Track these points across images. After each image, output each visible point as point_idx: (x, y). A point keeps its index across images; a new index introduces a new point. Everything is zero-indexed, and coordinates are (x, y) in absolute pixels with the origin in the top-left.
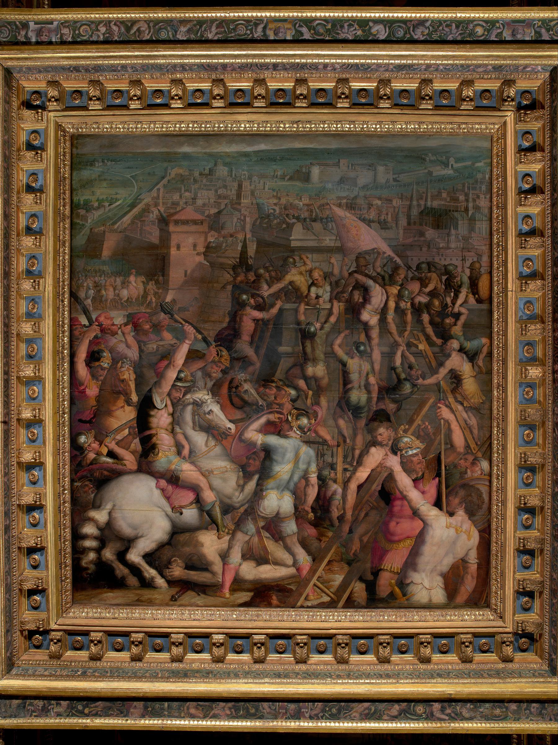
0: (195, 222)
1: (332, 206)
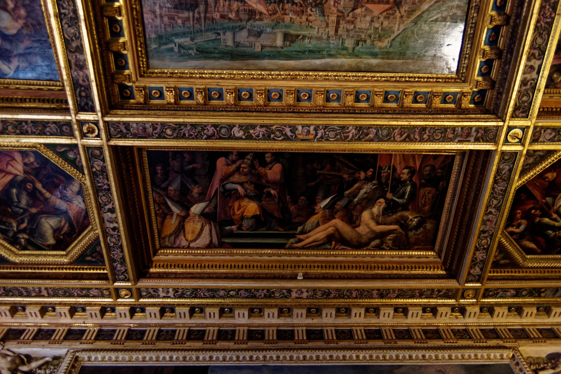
1: (267, 13)
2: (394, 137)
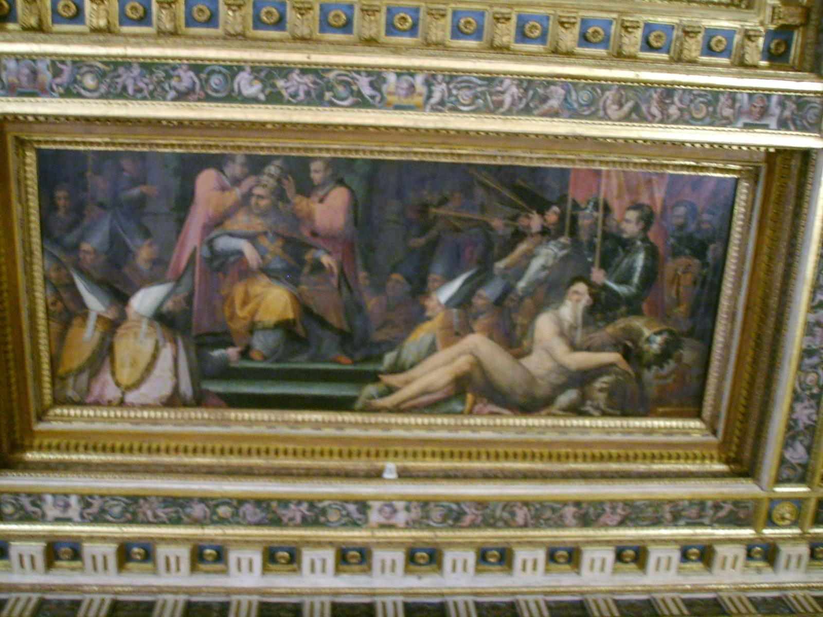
2: (605, 109)
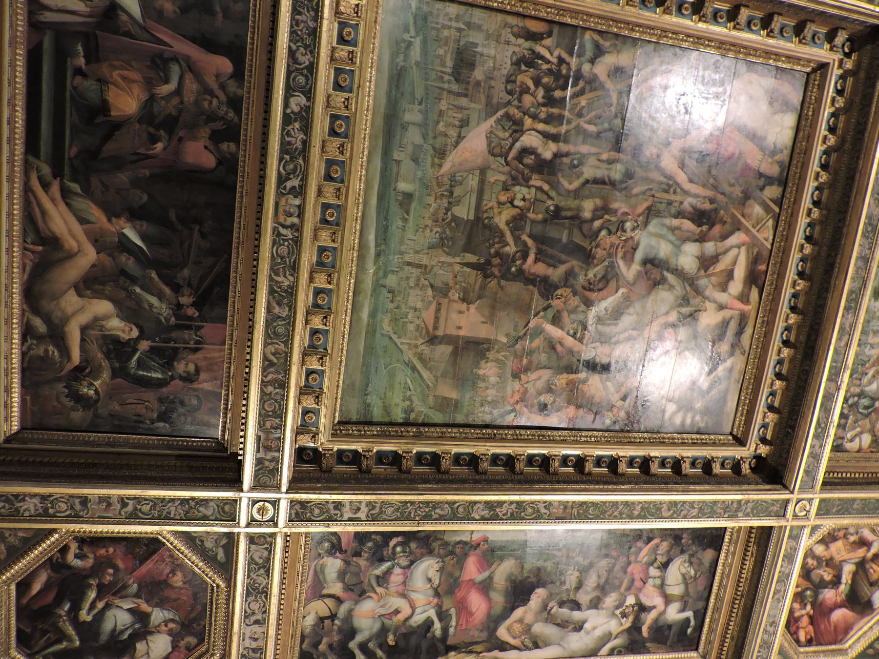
0: (438, 310)
2: (272, 344)
